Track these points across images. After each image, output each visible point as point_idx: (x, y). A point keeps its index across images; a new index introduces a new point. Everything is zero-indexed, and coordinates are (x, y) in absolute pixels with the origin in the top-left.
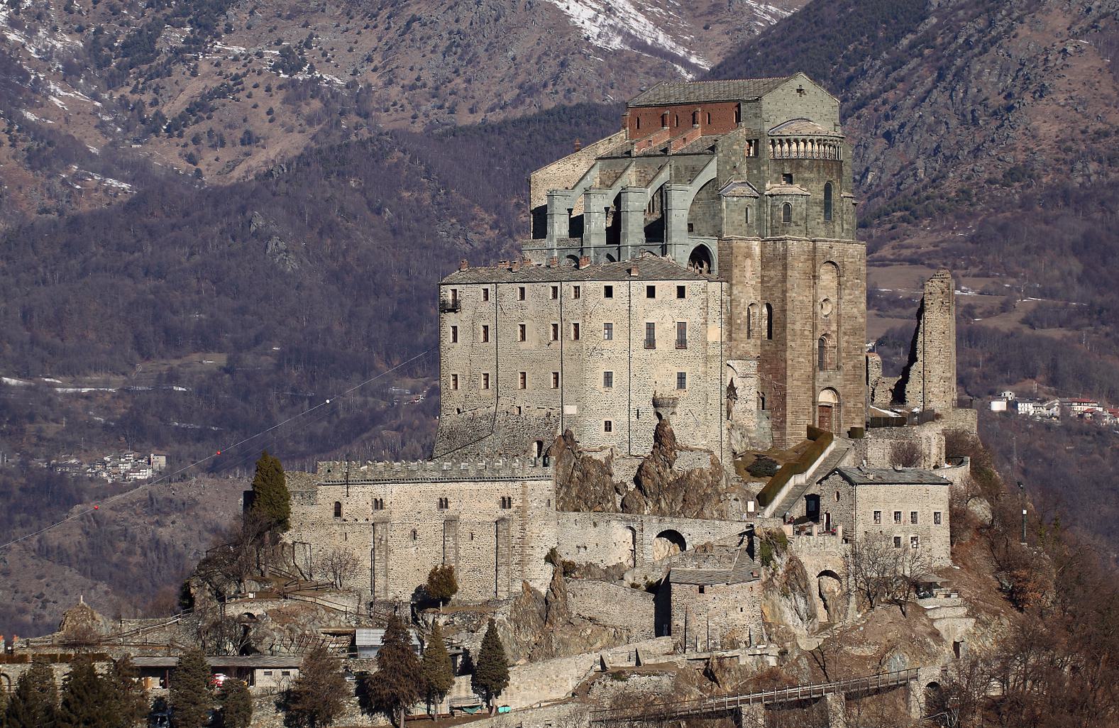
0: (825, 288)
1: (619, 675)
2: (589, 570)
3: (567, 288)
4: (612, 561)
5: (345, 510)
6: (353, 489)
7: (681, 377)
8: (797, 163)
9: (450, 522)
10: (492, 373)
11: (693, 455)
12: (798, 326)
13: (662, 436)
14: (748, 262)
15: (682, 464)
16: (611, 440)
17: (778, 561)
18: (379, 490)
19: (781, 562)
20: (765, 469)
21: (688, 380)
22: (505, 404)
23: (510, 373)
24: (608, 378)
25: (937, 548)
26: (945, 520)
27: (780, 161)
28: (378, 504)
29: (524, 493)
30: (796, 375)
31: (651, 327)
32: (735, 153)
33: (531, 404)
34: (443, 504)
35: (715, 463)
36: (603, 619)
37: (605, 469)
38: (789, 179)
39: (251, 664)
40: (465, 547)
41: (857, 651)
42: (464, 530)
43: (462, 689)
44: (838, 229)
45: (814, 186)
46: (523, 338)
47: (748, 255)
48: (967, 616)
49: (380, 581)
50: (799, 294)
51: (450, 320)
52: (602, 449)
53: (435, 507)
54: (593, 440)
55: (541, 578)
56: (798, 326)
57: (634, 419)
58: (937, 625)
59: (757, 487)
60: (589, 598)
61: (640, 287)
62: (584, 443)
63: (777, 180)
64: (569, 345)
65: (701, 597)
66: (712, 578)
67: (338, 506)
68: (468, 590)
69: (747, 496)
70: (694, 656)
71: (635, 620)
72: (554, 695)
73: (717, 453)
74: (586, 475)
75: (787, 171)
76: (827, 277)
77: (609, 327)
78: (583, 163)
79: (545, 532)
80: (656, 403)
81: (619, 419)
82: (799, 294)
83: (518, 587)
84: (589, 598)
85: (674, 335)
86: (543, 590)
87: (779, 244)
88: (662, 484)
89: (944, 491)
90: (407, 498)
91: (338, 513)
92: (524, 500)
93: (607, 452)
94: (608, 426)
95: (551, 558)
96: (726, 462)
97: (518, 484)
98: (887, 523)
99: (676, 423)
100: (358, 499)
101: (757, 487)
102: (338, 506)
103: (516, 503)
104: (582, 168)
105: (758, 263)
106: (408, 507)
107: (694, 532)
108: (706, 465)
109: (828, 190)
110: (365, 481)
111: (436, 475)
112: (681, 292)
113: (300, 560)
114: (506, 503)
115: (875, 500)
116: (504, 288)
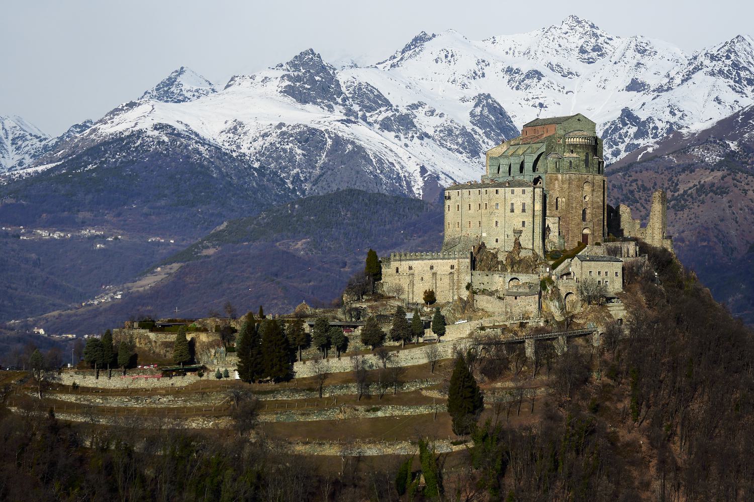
0: (586, 191)
1: (483, 328)
2: (484, 292)
3: (483, 190)
4: (494, 289)
5: (400, 270)
6: (403, 263)
7: (524, 223)
8: (575, 146)
9: (434, 274)
10: (460, 221)
11: (526, 251)
12: (574, 205)
13: (518, 245)
14: (557, 182)
15: (523, 254)
16: (497, 246)
17: (549, 288)
18: (411, 263)
19: (549, 288)
20: (557, 257)
21: (526, 224)
22: (464, 233)
23: (465, 221)
25: (615, 285)
27: (570, 145)
28: (410, 268)
29: (458, 264)
30: (573, 223)
31: (512, 204)
32: (553, 142)
33: (472, 232)
34: (432, 268)
36: (486, 309)
37: (495, 256)
38: (572, 152)
39: (358, 324)
40: (439, 283)
41: (578, 321)
42: (438, 277)
43: (429, 333)
44: (591, 170)
47: (557, 179)
48: (624, 310)
49: (411, 296)
50: (575, 193)
51: (448, 202)
52: (495, 248)
53: (429, 269)
54: (491, 245)
55: (465, 294)
56: (574, 205)
57: (506, 238)
59: (551, 263)
60: (482, 302)
61: (508, 190)
62: (488, 247)
63: (568, 152)
64: (483, 211)
66: (520, 294)
67: (397, 269)
68: (440, 299)
69: (547, 265)
70: (512, 322)
71: (496, 310)
72: (461, 336)
73: (537, 251)
74: (488, 257)
76: (587, 188)
77: (497, 204)
78: (505, 146)
79: (466, 278)
80: (515, 232)
81: (501, 238)
82: (575, 193)
83: (456, 298)
84: (482, 302)
85: (521, 207)
86: (465, 299)
87: (567, 175)
88: (516, 263)
89: (620, 265)
90: (420, 265)
91: (397, 271)
92: (459, 266)
93: (496, 250)
94: (497, 241)
95: (469, 287)
96: (540, 253)
97: (457, 260)
98: (594, 275)
99: (521, 240)
100: (404, 266)
101: (551, 263)
102: (397, 269)
103: (456, 267)
104: (505, 148)
106: (420, 269)
107: (524, 278)
108: (530, 254)
109: (587, 156)
110: (407, 260)
111: (429, 257)
112: (524, 192)
113: (385, 289)
114: (452, 267)
116: (464, 191)
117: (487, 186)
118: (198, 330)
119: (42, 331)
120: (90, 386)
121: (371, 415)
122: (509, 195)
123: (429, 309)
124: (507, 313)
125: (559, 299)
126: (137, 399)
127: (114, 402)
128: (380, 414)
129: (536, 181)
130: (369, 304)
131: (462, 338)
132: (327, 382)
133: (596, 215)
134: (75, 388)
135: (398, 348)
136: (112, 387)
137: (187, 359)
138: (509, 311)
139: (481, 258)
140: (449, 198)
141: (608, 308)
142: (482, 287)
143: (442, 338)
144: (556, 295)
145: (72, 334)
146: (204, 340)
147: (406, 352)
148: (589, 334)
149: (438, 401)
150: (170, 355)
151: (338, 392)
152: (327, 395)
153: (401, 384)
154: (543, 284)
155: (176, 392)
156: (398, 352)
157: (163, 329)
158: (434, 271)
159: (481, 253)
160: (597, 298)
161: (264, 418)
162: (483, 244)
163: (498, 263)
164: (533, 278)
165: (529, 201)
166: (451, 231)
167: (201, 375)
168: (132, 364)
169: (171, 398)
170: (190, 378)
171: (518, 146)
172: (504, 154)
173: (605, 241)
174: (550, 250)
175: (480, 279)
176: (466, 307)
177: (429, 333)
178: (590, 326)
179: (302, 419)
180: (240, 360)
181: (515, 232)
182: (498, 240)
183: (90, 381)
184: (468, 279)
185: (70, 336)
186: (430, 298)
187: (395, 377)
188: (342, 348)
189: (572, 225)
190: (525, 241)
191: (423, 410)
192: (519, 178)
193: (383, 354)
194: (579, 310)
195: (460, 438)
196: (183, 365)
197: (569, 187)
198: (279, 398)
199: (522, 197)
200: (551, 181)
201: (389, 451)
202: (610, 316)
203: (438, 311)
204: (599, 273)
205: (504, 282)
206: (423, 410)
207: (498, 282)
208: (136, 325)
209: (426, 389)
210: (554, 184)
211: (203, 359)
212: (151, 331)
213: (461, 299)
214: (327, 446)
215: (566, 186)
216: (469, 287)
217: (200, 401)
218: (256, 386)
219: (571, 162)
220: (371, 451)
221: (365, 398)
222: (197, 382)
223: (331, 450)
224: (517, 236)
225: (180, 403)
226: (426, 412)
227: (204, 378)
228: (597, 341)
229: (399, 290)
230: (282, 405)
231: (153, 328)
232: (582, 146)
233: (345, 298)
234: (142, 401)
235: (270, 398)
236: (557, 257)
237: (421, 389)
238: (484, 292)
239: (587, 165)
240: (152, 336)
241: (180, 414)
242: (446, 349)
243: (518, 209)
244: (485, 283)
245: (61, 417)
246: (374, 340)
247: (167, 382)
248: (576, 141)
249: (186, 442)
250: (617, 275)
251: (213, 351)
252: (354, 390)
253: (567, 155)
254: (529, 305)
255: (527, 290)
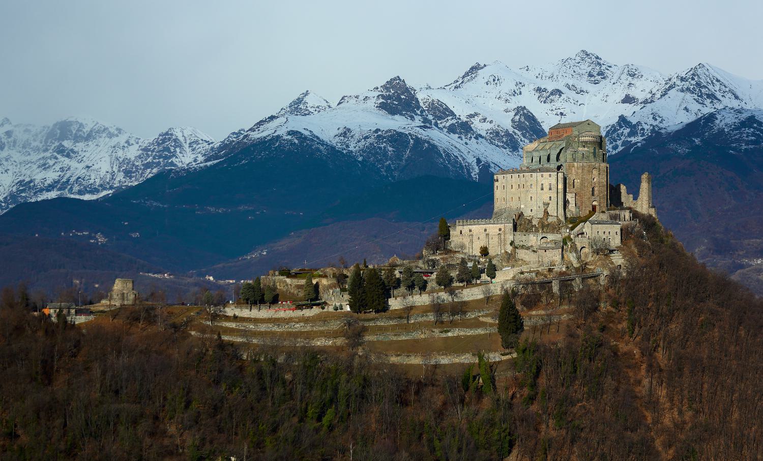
1: (522, 273)
2: (523, 247)
3: (521, 175)
5: (463, 232)
6: (465, 227)
7: (550, 197)
8: (586, 142)
13: (546, 213)
14: (573, 168)
15: (550, 220)
16: (532, 214)
17: (569, 244)
18: (470, 227)
19: (569, 244)
20: (574, 222)
24: (531, 197)
25: (616, 241)
26: (619, 233)
28: (470, 231)
33: (514, 205)
34: (485, 230)
35: (559, 221)
36: (524, 259)
37: (530, 221)
42: (490, 237)
43: (484, 277)
45: (590, 148)
46: (512, 188)
47: (574, 166)
49: (471, 250)
53: (483, 231)
54: (527, 214)
55: (509, 249)
56: (586, 185)
58: (613, 260)
61: (539, 174)
64: (522, 189)
65: (545, 253)
67: (461, 231)
68: (492, 252)
69: (567, 228)
72: (507, 279)
73: (560, 217)
75: (584, 144)
76: (595, 172)
80: (544, 204)
81: (535, 208)
83: (503, 251)
84: (521, 254)
86: (510, 252)
88: (545, 226)
91: (461, 233)
95: (512, 243)
96: (563, 219)
99: (549, 210)
100: (465, 229)
101: (570, 226)
102: (461, 231)
104: (536, 145)
105: (576, 167)
107: (551, 237)
108: (555, 220)
111: (484, 223)
112: (550, 176)
113: (452, 245)
114: (500, 230)
115: (598, 228)
117: (524, 171)
118: (320, 276)
119: (211, 278)
120: (246, 316)
121: (444, 335)
122: (539, 178)
123: (484, 260)
124: (539, 262)
125: (576, 251)
126: (279, 325)
127: (263, 328)
128: (450, 334)
129: (559, 168)
130: (441, 257)
131: (507, 280)
132: (412, 312)
133: (601, 191)
134: (235, 318)
135: (462, 288)
136: (261, 317)
137: (314, 297)
138: (541, 260)
139: (520, 223)
140: (497, 181)
141: (611, 258)
142: (521, 244)
143: (493, 280)
144: (574, 248)
145: (232, 279)
146: (325, 283)
147: (468, 290)
148: (597, 276)
149: (491, 325)
150: (301, 294)
151: (420, 319)
152: (412, 322)
153: (465, 313)
154: (565, 242)
155: (306, 320)
156: (462, 290)
157: (296, 276)
158: (487, 232)
159: (520, 219)
160: (603, 250)
161: (369, 338)
162: (522, 213)
163: (533, 226)
164: (558, 237)
165: (554, 182)
166: (498, 205)
167: (323, 308)
168: (275, 300)
169: (302, 324)
170: (316, 310)
171: (546, 143)
172: (536, 149)
173: (608, 210)
174: (569, 217)
175: (520, 238)
176: (510, 258)
177: (484, 277)
178: (598, 270)
179: (395, 338)
180: (350, 297)
181: (544, 204)
182: (532, 210)
183: (245, 313)
184: (511, 238)
185: (231, 281)
186: (485, 252)
187: (461, 308)
188: (423, 288)
189: (585, 199)
190: (552, 210)
191: (480, 331)
192: (547, 165)
193: (452, 292)
194: (590, 259)
195: (507, 351)
196: (311, 301)
197: (582, 172)
198: (379, 323)
199: (549, 179)
200: (570, 167)
201: (457, 360)
202: (612, 263)
203: (490, 261)
204: (604, 232)
205: (537, 240)
206: (480, 331)
207: (533, 239)
208: (277, 273)
209: (482, 316)
210: (572, 170)
211: (324, 297)
212: (288, 277)
213: (506, 252)
214: (413, 357)
215: (580, 171)
216: (512, 243)
217: (323, 326)
218: (362, 316)
219: (583, 154)
220: (444, 360)
221: (439, 323)
222: (321, 313)
223: (416, 360)
224: (546, 207)
225: (308, 328)
226: (483, 332)
227: (325, 310)
228: (603, 281)
229: (463, 246)
230: (382, 329)
231: (289, 275)
232: (591, 142)
233: (424, 252)
234: (282, 327)
235: (372, 324)
236: (574, 222)
237: (479, 317)
238: (523, 247)
239: (595, 156)
240: (288, 280)
241: (309, 335)
242: (496, 288)
243: (546, 187)
244: (524, 241)
245: (225, 338)
246: (445, 282)
247: (299, 313)
248: (587, 139)
249: (314, 355)
250: (617, 234)
251: (331, 291)
252: (431, 317)
253: (580, 149)
254: (555, 256)
255: (554, 246)
